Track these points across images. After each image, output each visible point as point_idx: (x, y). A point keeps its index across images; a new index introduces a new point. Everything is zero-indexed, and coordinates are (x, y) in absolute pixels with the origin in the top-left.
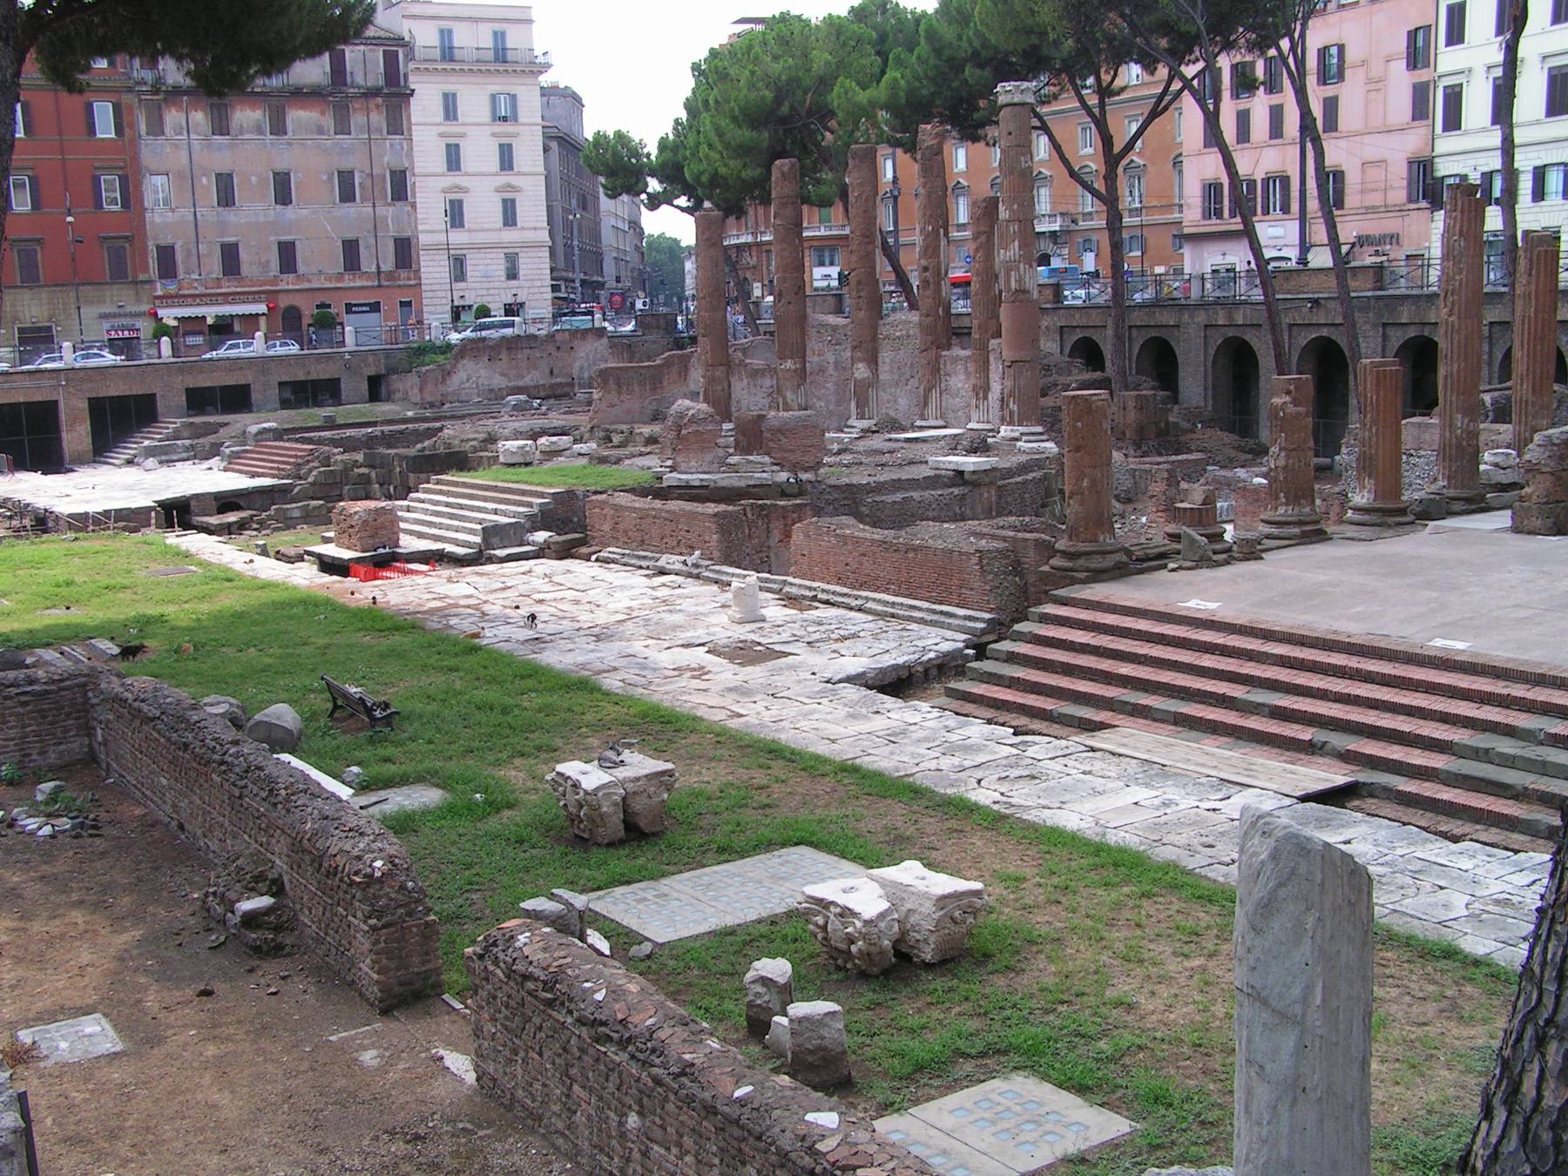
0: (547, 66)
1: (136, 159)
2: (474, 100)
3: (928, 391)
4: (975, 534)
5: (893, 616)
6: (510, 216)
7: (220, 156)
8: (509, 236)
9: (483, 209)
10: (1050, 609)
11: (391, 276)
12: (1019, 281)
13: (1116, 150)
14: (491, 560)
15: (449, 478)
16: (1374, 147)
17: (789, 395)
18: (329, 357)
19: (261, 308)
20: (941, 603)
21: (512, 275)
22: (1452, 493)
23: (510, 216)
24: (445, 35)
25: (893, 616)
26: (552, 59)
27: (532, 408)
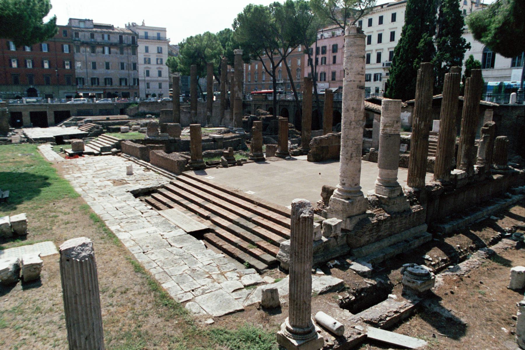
1: (73, 58)
3: (222, 118)
4: (182, 156)
6: (160, 74)
7: (93, 58)
8: (160, 79)
9: (154, 72)
10: (181, 177)
11: (132, 87)
12: (238, 95)
14: (101, 155)
19: (102, 92)
21: (160, 87)
23: (160, 74)
24: (146, 33)
26: (171, 40)
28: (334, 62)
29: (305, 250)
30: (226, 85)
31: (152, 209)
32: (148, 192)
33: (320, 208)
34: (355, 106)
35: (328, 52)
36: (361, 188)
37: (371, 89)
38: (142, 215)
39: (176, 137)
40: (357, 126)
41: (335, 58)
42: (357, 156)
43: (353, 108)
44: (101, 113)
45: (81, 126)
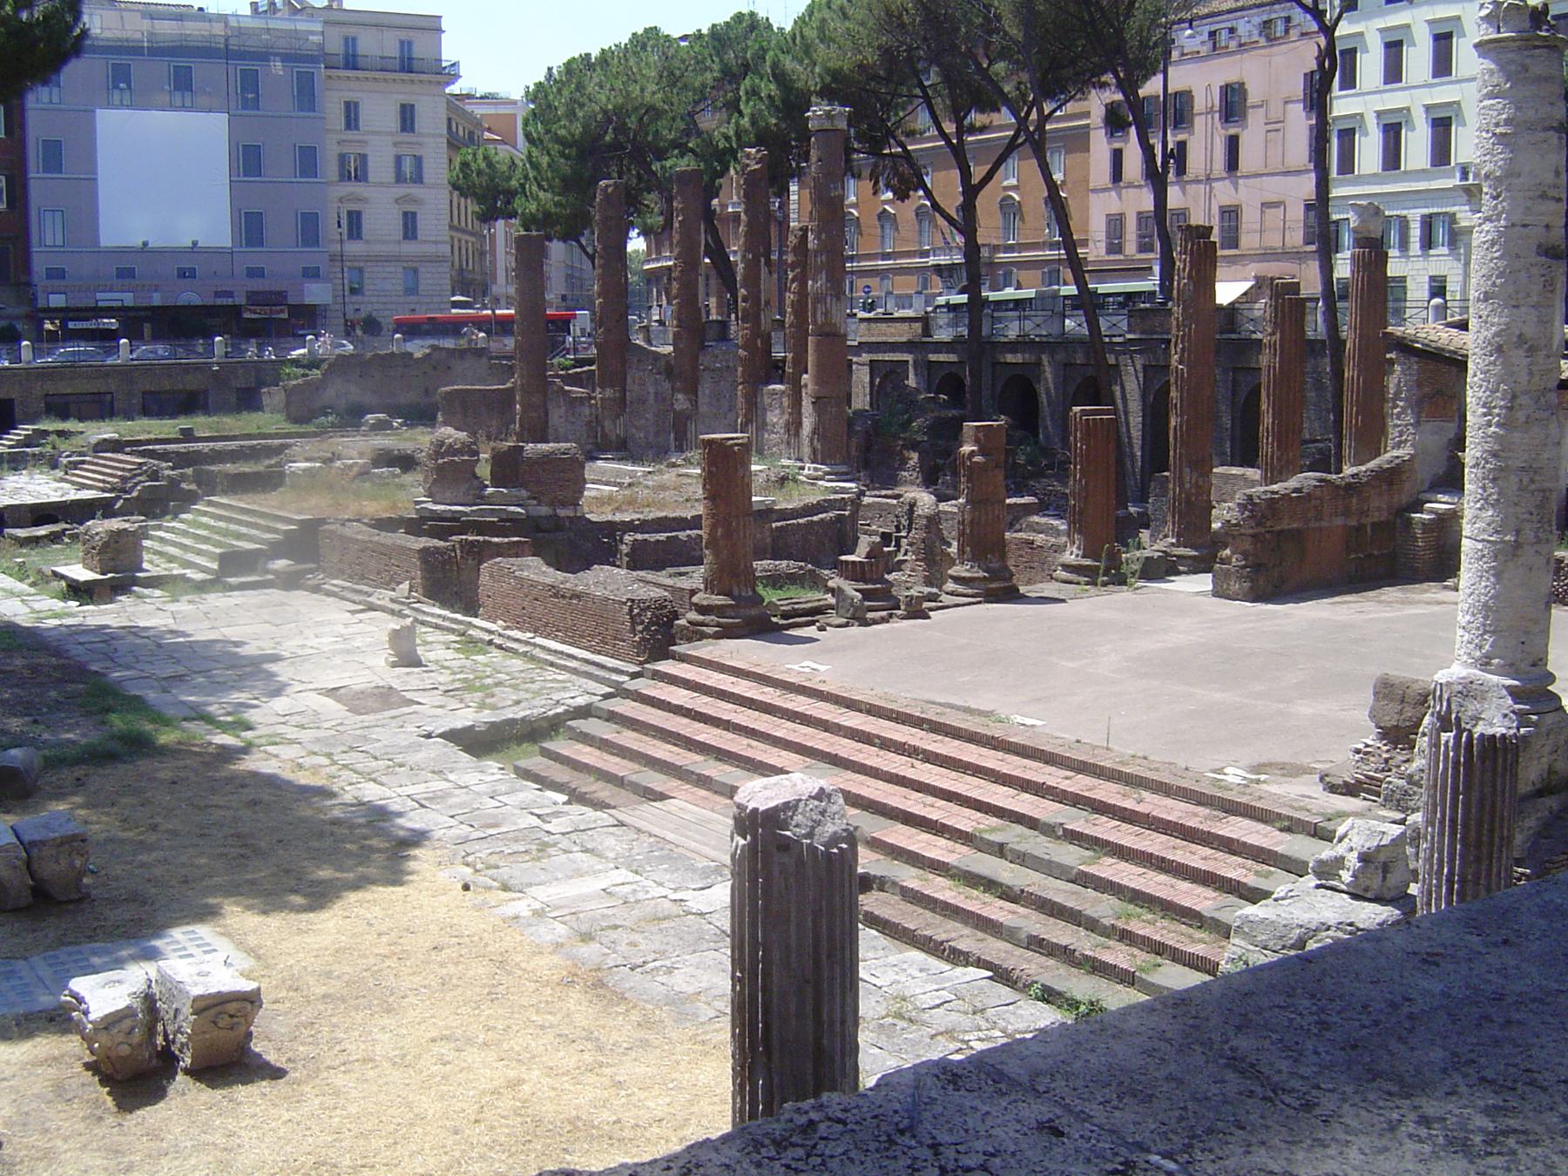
0: (457, 77)
2: (379, 112)
5: (552, 664)
6: (410, 226)
8: (410, 248)
10: (665, 666)
13: (975, 180)
15: (224, 500)
16: (1274, 188)
17: (607, 424)
18: (197, 368)
20: (599, 653)
22: (1181, 551)
23: (410, 226)
24: (350, 42)
25: (552, 664)
27: (391, 428)
28: (1232, 163)
29: (1489, 870)
30: (764, 270)
31: (568, 803)
32: (534, 732)
33: (1370, 769)
34: (1530, 331)
35: (1199, 122)
36: (1551, 678)
37: (1410, 284)
38: (547, 827)
39: (564, 505)
40: (1539, 414)
41: (1233, 144)
42: (1539, 541)
43: (1520, 336)
44: (155, 406)
45: (75, 465)
